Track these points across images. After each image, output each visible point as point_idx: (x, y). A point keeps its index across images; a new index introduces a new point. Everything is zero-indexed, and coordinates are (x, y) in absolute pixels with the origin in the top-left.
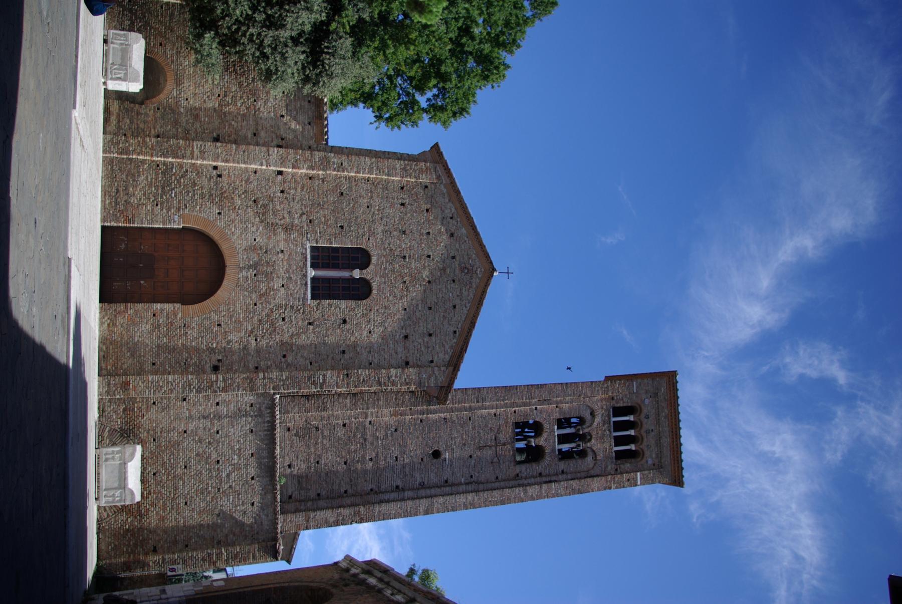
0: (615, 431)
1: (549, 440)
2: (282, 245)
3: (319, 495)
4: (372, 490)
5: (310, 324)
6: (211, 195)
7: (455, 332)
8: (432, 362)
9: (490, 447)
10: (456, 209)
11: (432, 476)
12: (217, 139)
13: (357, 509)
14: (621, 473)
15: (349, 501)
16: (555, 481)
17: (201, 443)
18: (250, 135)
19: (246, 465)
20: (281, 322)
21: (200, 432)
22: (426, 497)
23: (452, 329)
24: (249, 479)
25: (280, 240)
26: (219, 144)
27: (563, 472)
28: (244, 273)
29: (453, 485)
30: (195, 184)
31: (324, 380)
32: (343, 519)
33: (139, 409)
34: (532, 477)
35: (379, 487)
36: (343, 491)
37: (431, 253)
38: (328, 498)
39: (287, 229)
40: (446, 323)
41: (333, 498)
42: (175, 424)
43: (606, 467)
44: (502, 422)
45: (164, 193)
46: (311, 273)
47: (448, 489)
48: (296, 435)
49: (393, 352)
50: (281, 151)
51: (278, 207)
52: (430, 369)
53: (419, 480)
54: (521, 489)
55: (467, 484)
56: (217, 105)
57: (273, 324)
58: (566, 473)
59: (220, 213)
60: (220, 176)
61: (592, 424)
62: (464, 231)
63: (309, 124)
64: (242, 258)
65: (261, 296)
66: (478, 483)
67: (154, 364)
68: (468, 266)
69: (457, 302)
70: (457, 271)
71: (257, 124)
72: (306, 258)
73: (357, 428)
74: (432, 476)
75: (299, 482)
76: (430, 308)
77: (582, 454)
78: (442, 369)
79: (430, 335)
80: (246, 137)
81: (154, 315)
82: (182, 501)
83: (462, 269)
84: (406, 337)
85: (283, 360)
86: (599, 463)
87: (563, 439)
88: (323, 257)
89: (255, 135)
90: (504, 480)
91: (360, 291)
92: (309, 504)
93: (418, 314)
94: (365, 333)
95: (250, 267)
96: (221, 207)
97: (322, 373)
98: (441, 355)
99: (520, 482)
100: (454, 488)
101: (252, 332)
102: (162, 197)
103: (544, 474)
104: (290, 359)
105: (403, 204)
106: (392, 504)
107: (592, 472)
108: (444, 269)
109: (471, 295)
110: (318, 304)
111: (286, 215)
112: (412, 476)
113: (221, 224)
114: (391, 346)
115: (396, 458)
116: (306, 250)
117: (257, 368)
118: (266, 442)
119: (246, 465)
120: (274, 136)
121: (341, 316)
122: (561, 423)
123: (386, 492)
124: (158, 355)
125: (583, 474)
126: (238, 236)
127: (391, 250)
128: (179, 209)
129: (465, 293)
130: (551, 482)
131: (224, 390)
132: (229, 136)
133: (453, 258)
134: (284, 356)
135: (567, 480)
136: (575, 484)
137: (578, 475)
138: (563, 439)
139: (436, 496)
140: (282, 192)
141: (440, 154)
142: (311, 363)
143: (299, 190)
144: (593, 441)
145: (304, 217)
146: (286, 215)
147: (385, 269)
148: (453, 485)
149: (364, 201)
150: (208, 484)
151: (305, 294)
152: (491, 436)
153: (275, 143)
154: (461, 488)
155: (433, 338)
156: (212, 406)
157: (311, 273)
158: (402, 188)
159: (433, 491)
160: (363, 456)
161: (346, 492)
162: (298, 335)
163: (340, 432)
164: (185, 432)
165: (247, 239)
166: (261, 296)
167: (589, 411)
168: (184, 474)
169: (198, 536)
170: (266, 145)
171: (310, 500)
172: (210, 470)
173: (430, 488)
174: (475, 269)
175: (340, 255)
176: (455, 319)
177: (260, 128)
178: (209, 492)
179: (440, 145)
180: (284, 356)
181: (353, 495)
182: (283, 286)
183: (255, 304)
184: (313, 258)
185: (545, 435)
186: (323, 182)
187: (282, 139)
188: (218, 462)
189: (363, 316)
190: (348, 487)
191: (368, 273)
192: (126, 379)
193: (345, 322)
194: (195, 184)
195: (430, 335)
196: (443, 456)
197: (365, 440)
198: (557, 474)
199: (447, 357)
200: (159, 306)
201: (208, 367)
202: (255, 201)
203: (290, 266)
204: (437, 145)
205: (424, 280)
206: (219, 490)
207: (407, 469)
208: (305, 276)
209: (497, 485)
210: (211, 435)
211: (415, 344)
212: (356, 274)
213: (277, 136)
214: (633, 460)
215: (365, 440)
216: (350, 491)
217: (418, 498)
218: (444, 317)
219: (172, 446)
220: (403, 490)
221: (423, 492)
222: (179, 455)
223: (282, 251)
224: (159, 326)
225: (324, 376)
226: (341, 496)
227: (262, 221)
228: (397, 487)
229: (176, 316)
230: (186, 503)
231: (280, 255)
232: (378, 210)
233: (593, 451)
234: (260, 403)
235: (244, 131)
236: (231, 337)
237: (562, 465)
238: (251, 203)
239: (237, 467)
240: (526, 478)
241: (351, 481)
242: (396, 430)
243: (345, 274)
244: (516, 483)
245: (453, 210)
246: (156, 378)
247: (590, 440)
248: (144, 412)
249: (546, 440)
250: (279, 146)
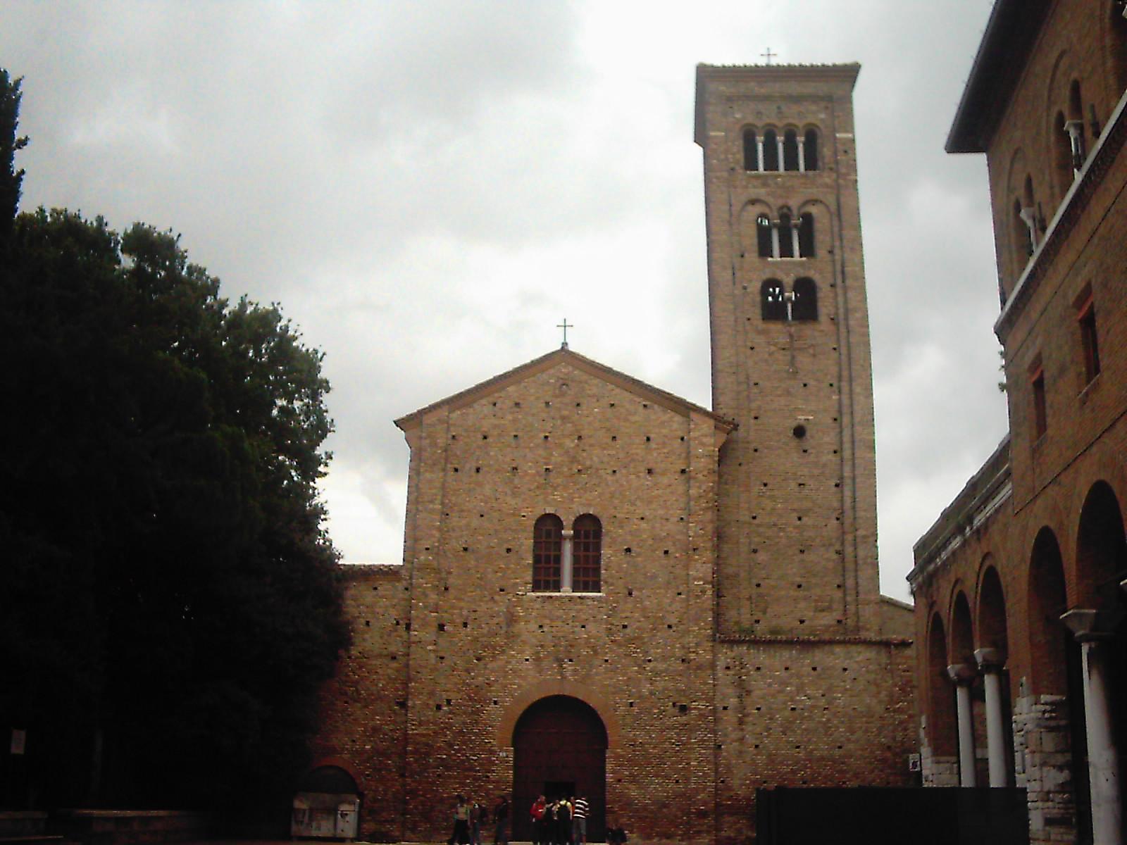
0: (777, 169)
1: (788, 267)
2: (533, 626)
3: (839, 586)
4: (838, 519)
5: (630, 594)
6: (473, 713)
7: (645, 406)
8: (682, 439)
9: (793, 357)
10: (481, 398)
11: (827, 439)
12: (403, 705)
13: (858, 540)
14: (837, 162)
15: (849, 550)
16: (843, 267)
17: (771, 729)
18: (395, 665)
19: (799, 676)
20: (628, 631)
21: (758, 730)
22: (853, 449)
23: (641, 408)
24: (815, 673)
25: (527, 629)
26: (410, 703)
27: (831, 252)
28: (568, 674)
29: (840, 412)
30: (461, 731)
31: (699, 579)
32: (872, 557)
33: (730, 798)
34: (836, 295)
35: (835, 510)
36: (835, 556)
37: (542, 435)
38: (844, 576)
39: (512, 619)
40: (634, 419)
41: (844, 569)
42: (748, 759)
43: (827, 186)
44: (760, 340)
45: (472, 769)
46: (566, 591)
47: (846, 420)
48: (764, 612)
49: (668, 490)
50: (415, 625)
51: (485, 631)
52: (692, 443)
53: (831, 457)
54: (850, 316)
55: (840, 392)
56: (359, 705)
57: (632, 640)
58: (833, 247)
59: (495, 703)
60: (449, 701)
61: (767, 205)
62: (511, 389)
63: (376, 589)
64: (551, 675)
65: (596, 653)
66: (840, 378)
67: (677, 782)
68: (559, 384)
69: (605, 402)
70: (566, 400)
71: (380, 656)
72: (551, 597)
73: (760, 535)
74: (827, 439)
75: (823, 611)
76: (614, 438)
77: (808, 219)
78: (692, 426)
79: (648, 439)
80: (398, 670)
81: (620, 781)
82: (837, 752)
83: (563, 394)
84: (650, 471)
85: (674, 629)
86: (821, 197)
87: (786, 251)
88: (545, 576)
89: (394, 658)
90: (838, 341)
91: (589, 529)
92: (849, 599)
93: (621, 455)
94: (643, 525)
95: (561, 666)
96: (485, 701)
97: (692, 581)
98: (675, 426)
99: (841, 316)
100: (846, 410)
101: (639, 666)
102: (479, 771)
103: (832, 281)
104: (673, 621)
105: (478, 470)
106: (858, 494)
107: (833, 208)
108: (563, 418)
109: (596, 381)
110: (606, 582)
111: (496, 620)
112: (825, 465)
113: (508, 701)
114: (660, 492)
115: (800, 485)
116: (538, 597)
117: (683, 661)
118: (772, 652)
119: (799, 676)
120: (395, 634)
121: (622, 556)
122: (765, 251)
123: (842, 501)
124: (667, 777)
125: (836, 223)
126: (522, 678)
127: (538, 487)
128: (492, 753)
129: (595, 390)
130: (843, 272)
131: (710, 700)
132: (397, 689)
133: (547, 403)
134: (670, 627)
135: (842, 247)
136: (847, 234)
137: (836, 229)
138: (786, 251)
139: (853, 436)
140: (465, 625)
141: (411, 418)
142: (679, 594)
143: (462, 604)
144: (794, 203)
145: (497, 597)
146: (496, 620)
147: (562, 497)
148: (840, 412)
149: (476, 522)
150: (820, 722)
151: (593, 599)
152: (780, 356)
153: (404, 634)
154: (846, 401)
155: (652, 436)
156: (726, 716)
157: (566, 591)
158: (456, 470)
159: (846, 438)
160: (796, 527)
161: (838, 552)
162: (644, 609)
163: (762, 557)
164: (757, 746)
165: (528, 670)
166: (596, 653)
167: (750, 208)
168: (805, 749)
169: (878, 735)
170: (408, 644)
171: (844, 598)
172: (803, 718)
173: (841, 443)
174: (562, 376)
175: (543, 553)
176: (628, 406)
177: (385, 652)
178: (829, 720)
179: (395, 419)
180: (670, 627)
181: (843, 544)
182: (583, 627)
183: (606, 661)
184: (546, 588)
185: (780, 275)
186: (450, 573)
187: (398, 623)
188: (793, 709)
189: (622, 527)
190: (832, 550)
191: (568, 520)
192: (693, 813)
193: (628, 550)
194: (461, 731)
195: (648, 439)
196: (802, 422)
197: (775, 525)
198: (833, 261)
199: (678, 418)
200: (609, 777)
201: (684, 719)
202: (478, 659)
203: (558, 617)
204: (398, 423)
205: (578, 445)
206: (825, 709)
207: (816, 472)
208: (571, 599)
209: (844, 351)
210: (761, 716)
211: (659, 460)
212: (568, 532)
213: (396, 631)
214: (819, 141)
215: (775, 525)
216: (837, 547)
217: (853, 459)
218: (626, 420)
219: (773, 762)
220: (841, 478)
221: (847, 453)
222: (783, 754)
223: (541, 627)
224: (631, 775)
225: (695, 579)
226: (843, 560)
227: (503, 652)
228: (837, 485)
229: (622, 756)
230: (840, 747)
231: (545, 629)
232: (486, 503)
233: (807, 203)
234: (726, 658)
235: (389, 671)
236: (645, 691)
237: (821, 252)
238: (481, 664)
239: (800, 689)
240: (837, 308)
241: (824, 545)
242: (765, 485)
243: (568, 548)
244: (842, 322)
245: (484, 401)
246: (694, 779)
247: (789, 209)
248: (732, 793)
249: (788, 275)
250: (408, 627)
